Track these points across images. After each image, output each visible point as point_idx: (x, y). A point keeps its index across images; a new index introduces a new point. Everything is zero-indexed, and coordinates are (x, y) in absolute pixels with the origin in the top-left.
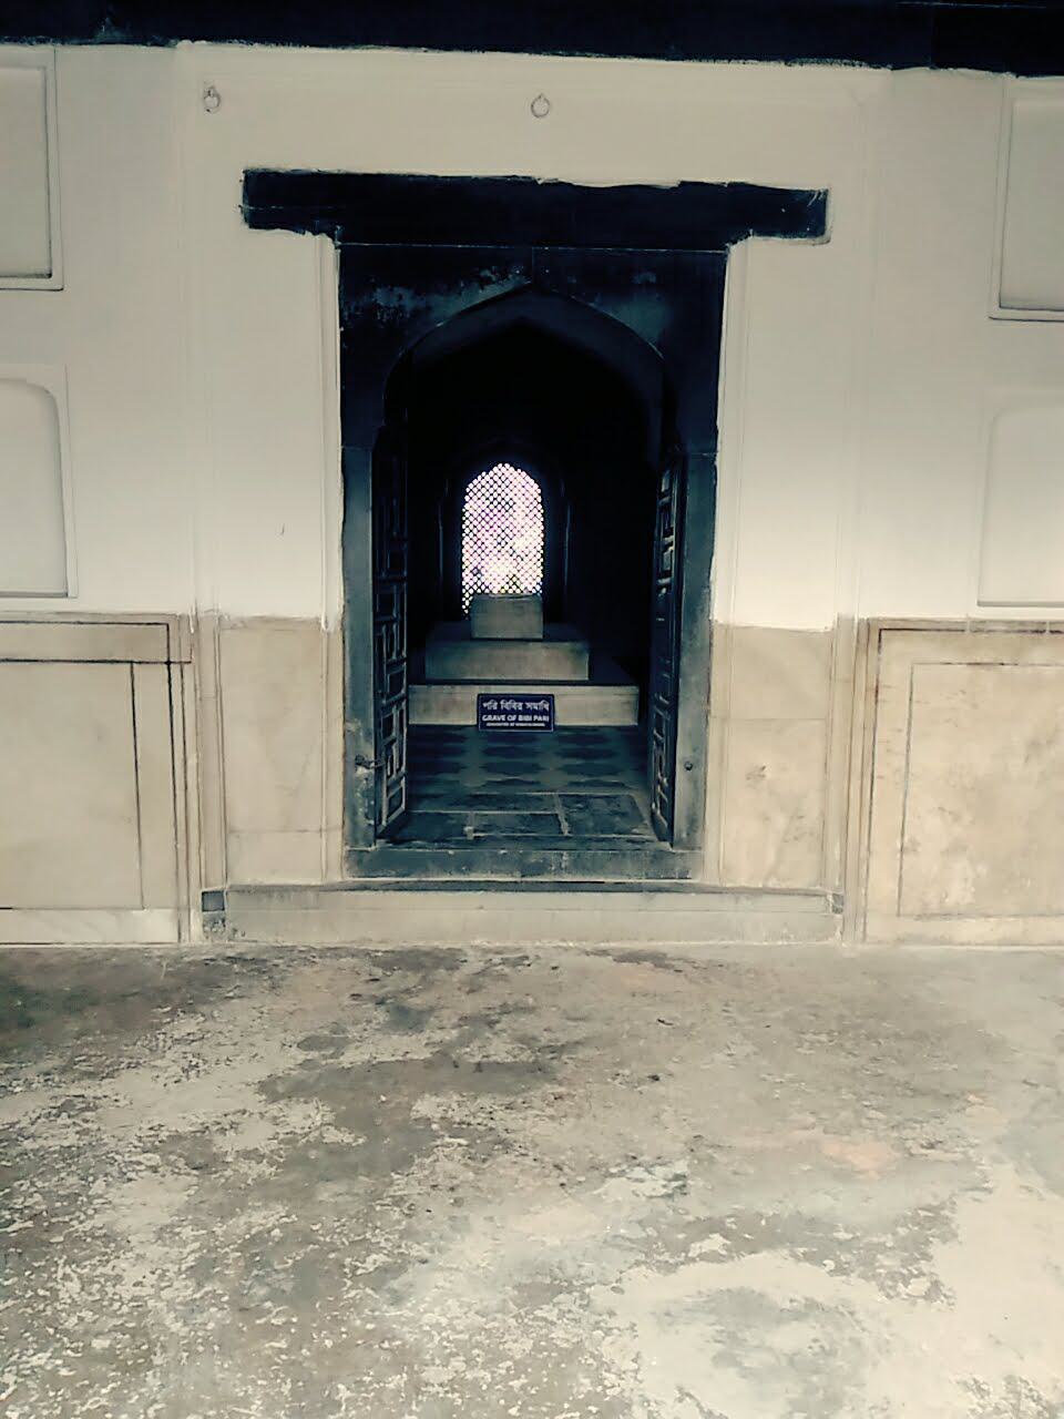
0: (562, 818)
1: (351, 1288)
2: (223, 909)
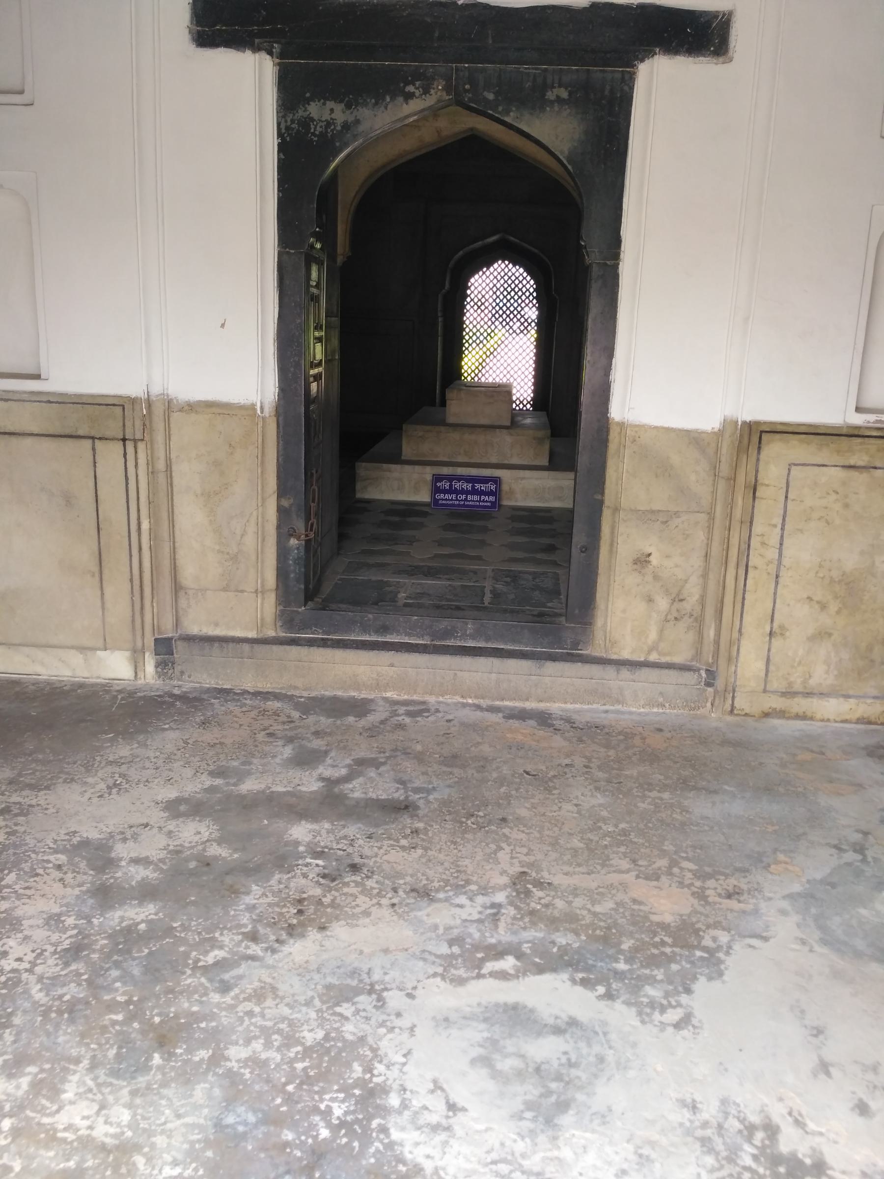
1: (190, 976)
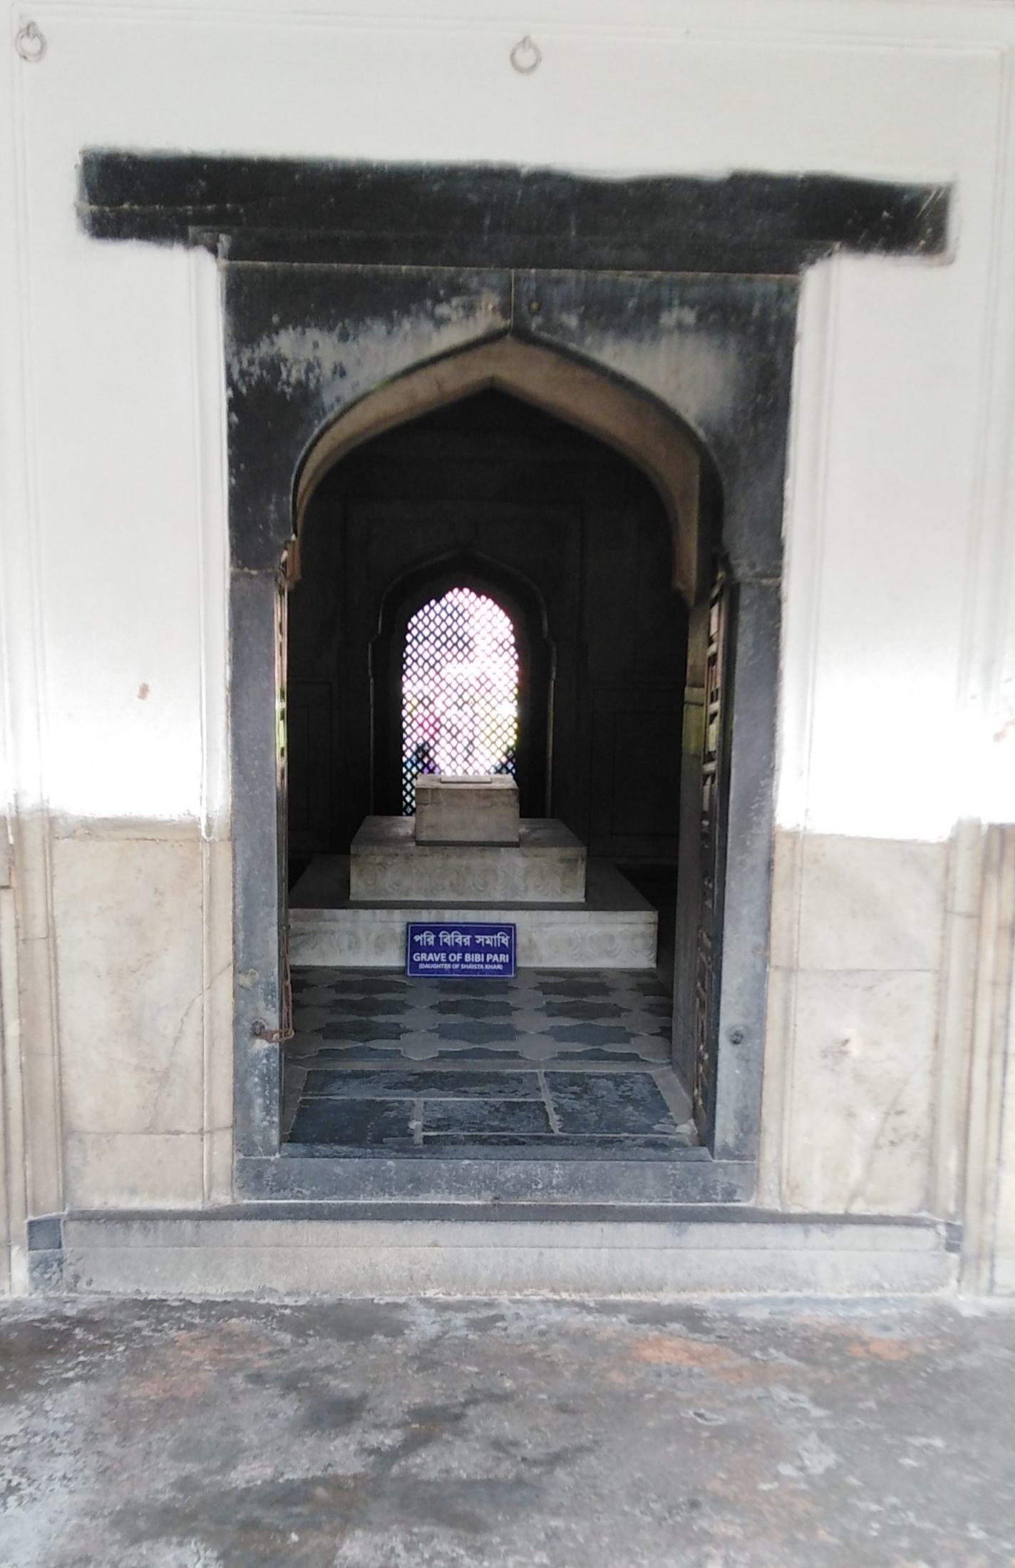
0: (550, 1108)
2: (60, 1247)
